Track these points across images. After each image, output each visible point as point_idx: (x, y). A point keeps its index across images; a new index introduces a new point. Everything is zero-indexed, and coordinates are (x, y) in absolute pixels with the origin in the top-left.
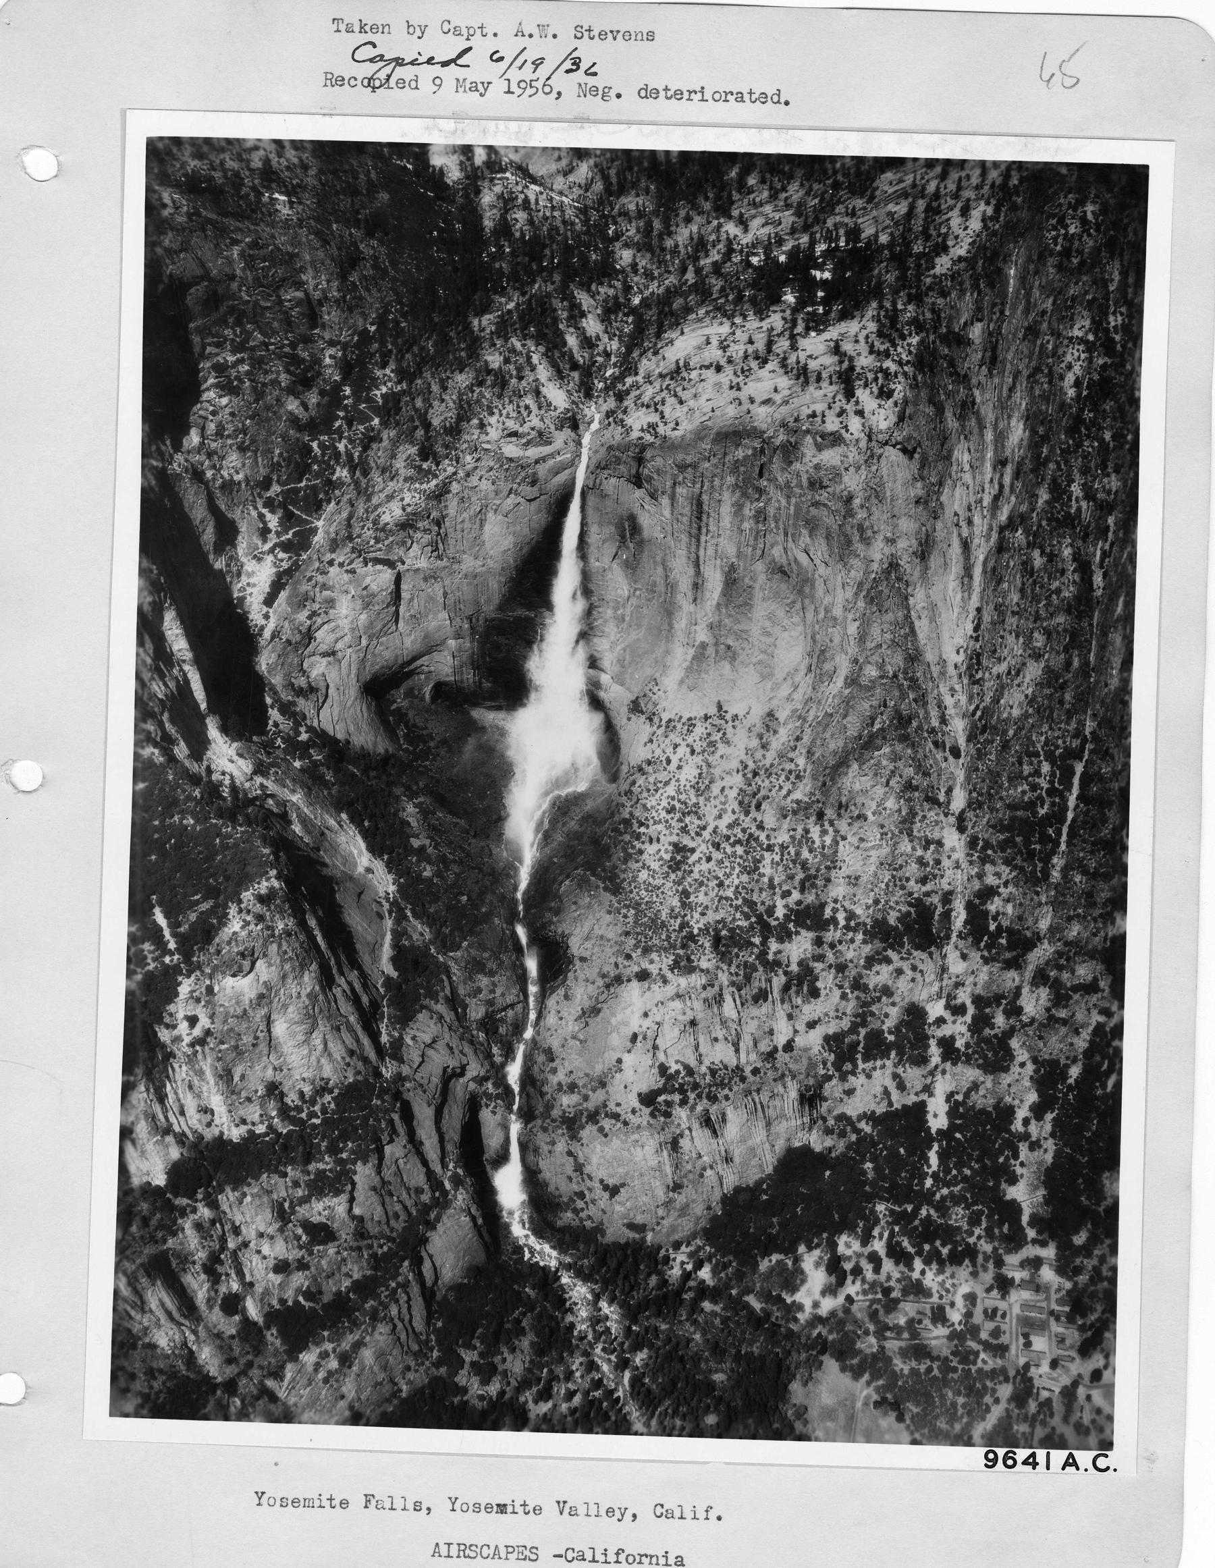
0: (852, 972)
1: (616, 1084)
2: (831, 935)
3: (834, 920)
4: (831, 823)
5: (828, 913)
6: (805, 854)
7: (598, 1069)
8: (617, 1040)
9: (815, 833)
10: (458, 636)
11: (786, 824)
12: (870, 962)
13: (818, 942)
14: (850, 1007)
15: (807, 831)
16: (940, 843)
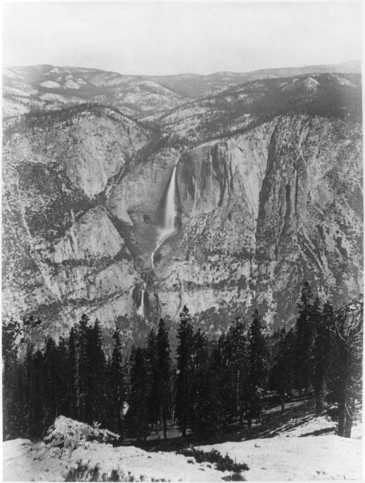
0: (227, 265)
1: (167, 281)
2: (223, 256)
3: (224, 253)
4: (225, 232)
5: (223, 251)
6: (218, 237)
7: (164, 277)
8: (170, 272)
9: (221, 234)
10: (149, 202)
11: (214, 232)
12: (232, 263)
13: (220, 257)
14: (228, 273)
15: (219, 233)
16: (251, 238)
